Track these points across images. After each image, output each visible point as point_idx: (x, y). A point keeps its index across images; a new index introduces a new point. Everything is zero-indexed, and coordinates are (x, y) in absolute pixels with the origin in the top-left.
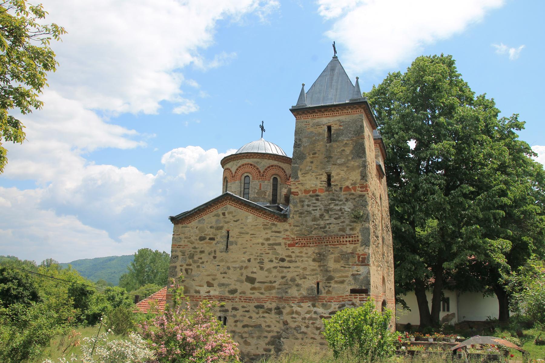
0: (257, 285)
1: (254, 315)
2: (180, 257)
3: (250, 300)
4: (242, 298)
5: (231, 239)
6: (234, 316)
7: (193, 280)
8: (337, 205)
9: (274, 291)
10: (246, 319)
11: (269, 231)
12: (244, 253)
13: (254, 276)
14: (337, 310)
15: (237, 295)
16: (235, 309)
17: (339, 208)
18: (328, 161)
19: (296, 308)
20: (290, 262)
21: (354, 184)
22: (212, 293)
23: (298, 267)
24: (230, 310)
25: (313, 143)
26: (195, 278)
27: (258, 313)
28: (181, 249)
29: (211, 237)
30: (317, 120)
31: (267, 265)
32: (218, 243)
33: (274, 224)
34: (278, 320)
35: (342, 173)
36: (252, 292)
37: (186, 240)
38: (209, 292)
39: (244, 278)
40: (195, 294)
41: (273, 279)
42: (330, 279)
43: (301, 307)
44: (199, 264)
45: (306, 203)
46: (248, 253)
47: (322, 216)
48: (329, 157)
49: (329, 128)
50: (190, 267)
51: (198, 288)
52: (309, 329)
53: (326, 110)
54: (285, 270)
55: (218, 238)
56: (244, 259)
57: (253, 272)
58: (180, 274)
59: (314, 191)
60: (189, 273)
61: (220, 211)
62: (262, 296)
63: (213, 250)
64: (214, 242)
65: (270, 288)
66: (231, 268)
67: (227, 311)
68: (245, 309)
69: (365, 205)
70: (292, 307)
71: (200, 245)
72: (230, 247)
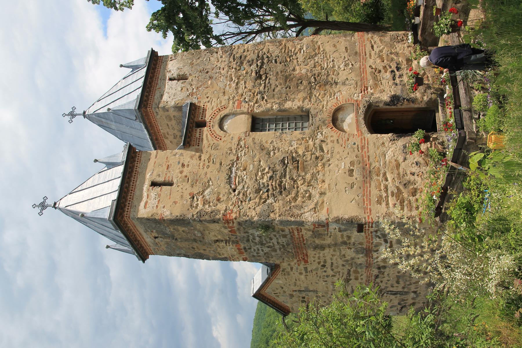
5: (303, 289)
8: (254, 239)
10: (389, 282)
11: (291, 273)
14: (382, 239)
17: (257, 239)
18: (200, 241)
21: (225, 228)
25: (180, 248)
30: (150, 243)
35: (212, 234)
45: (255, 254)
47: (268, 247)
48: (195, 240)
49: (156, 238)
53: (136, 240)
55: (303, 295)
59: (239, 249)
61: (273, 296)
69: (250, 223)
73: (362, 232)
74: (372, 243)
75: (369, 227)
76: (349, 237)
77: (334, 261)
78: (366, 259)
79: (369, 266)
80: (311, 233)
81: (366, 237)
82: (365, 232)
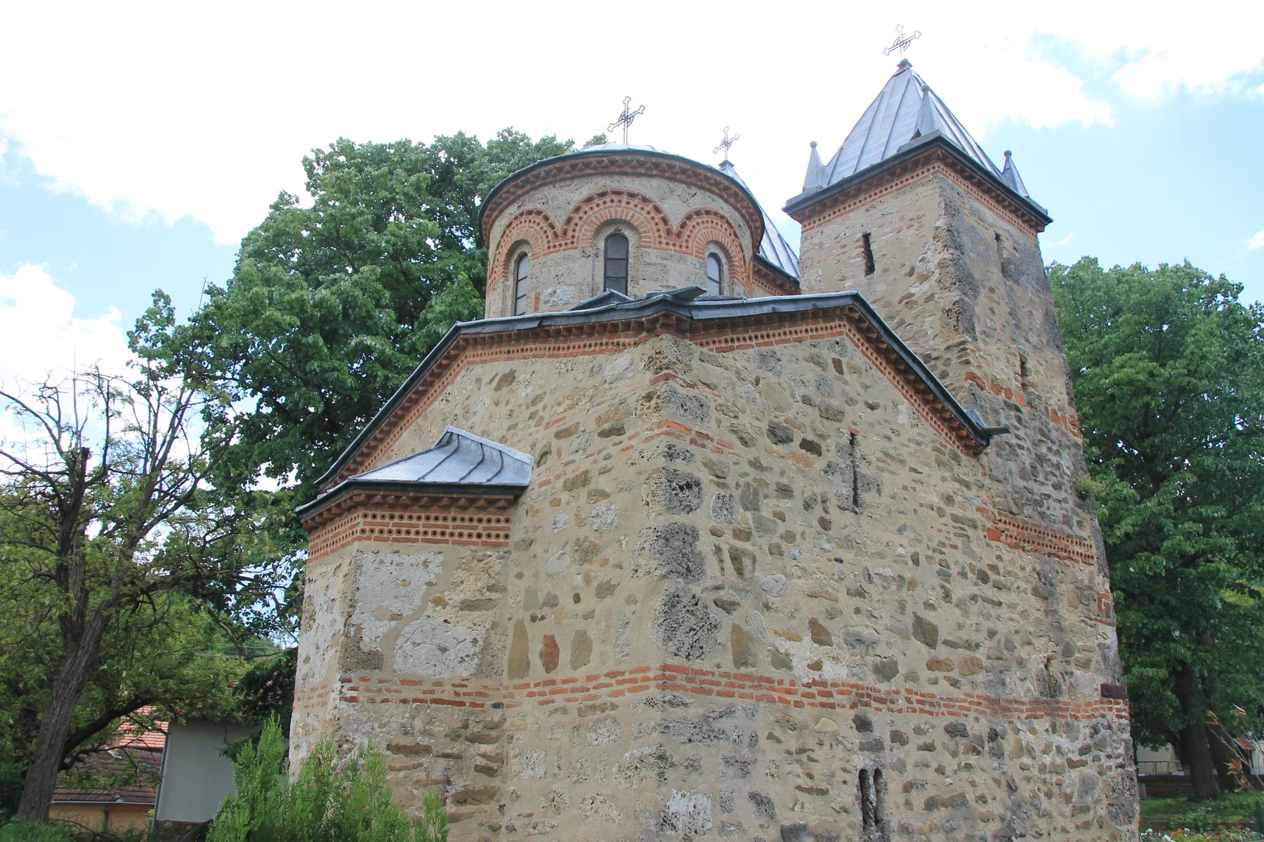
0: (942, 652)
1: (950, 763)
2: (710, 492)
3: (927, 704)
4: (914, 698)
6: (900, 767)
7: (767, 607)
9: (980, 677)
10: (930, 775)
12: (901, 530)
13: (930, 616)
14: (1088, 741)
15: (898, 683)
16: (898, 738)
19: (1026, 737)
20: (999, 587)
22: (830, 672)
23: (1012, 606)
24: (887, 742)
26: (771, 599)
27: (955, 754)
28: (708, 453)
29: (810, 437)
31: (962, 589)
32: (829, 469)
33: (955, 457)
34: (997, 774)
36: (933, 674)
37: (726, 422)
38: (817, 666)
39: (909, 621)
40: (777, 674)
41: (975, 637)
42: (1068, 652)
43: (1033, 731)
44: (776, 539)
46: (909, 534)
50: (747, 546)
51: (783, 645)
52: (1054, 800)
54: (994, 611)
56: (900, 550)
57: (930, 606)
58: (712, 567)
60: (747, 574)
62: (956, 693)
63: (818, 490)
64: (819, 463)
65: (972, 666)
66: (876, 579)
67: (876, 747)
68: (922, 740)
70: (1019, 730)
71: (783, 462)
72: (864, 496)
73: (1103, 695)
74: (1076, 718)
75: (1118, 710)
76: (1085, 665)
77: (1004, 612)
78: (1025, 700)
79: (999, 706)
80: (1086, 582)
81: (1089, 704)
82: (1102, 702)
